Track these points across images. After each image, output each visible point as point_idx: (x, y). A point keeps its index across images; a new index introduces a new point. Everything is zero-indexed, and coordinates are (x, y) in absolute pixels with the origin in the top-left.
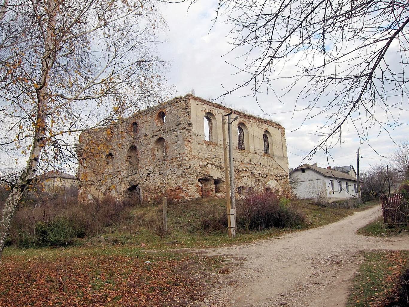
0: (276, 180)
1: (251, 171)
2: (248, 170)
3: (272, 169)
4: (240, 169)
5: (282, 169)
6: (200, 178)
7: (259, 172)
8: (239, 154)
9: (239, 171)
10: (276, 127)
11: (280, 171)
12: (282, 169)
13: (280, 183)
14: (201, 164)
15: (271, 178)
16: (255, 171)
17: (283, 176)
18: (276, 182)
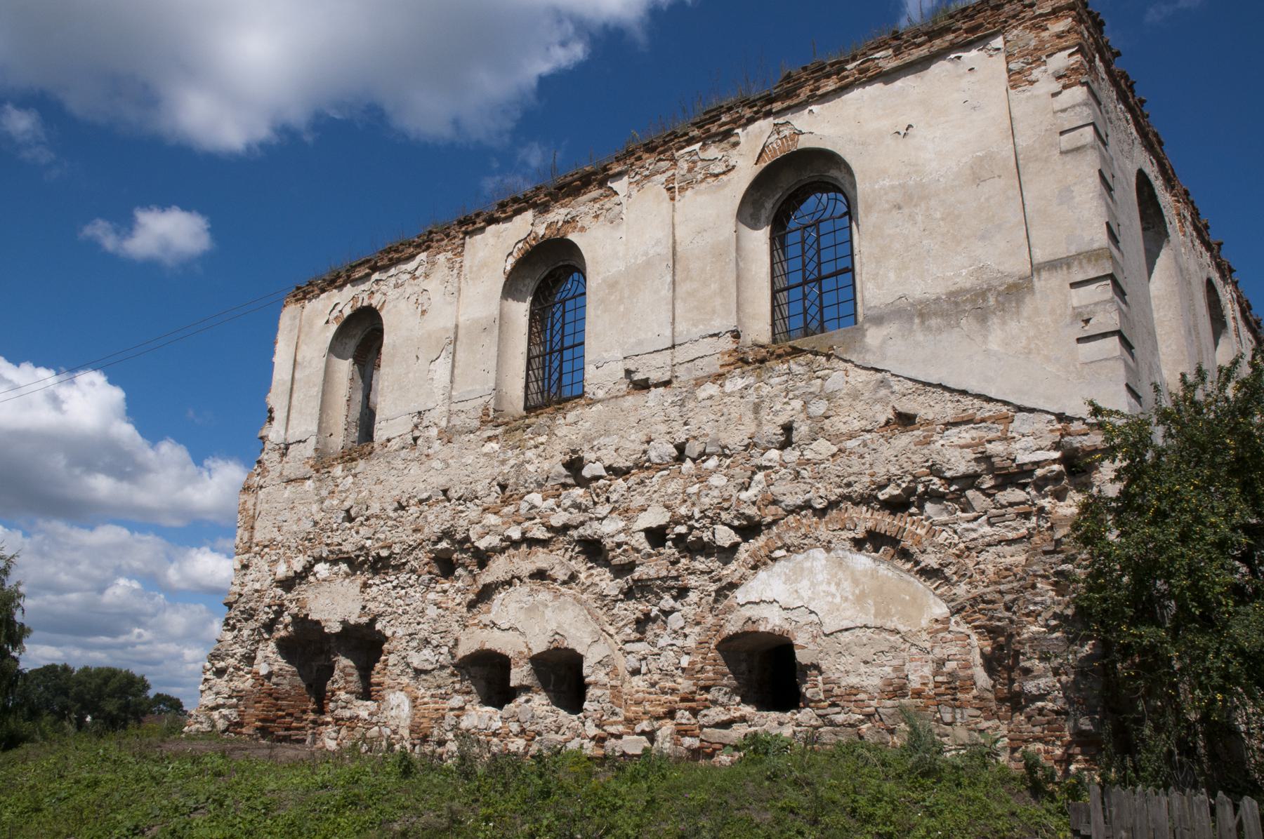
0: (873, 540)
1: (575, 534)
2: (540, 533)
3: (823, 447)
4: (482, 544)
5: (989, 410)
6: (283, 633)
7: (655, 517)
8: (494, 445)
9: (483, 558)
10: (916, 53)
11: (966, 434)
12: (989, 410)
13: (931, 561)
14: (282, 571)
15: (791, 538)
16: (609, 528)
17: (1013, 476)
18: (863, 561)
